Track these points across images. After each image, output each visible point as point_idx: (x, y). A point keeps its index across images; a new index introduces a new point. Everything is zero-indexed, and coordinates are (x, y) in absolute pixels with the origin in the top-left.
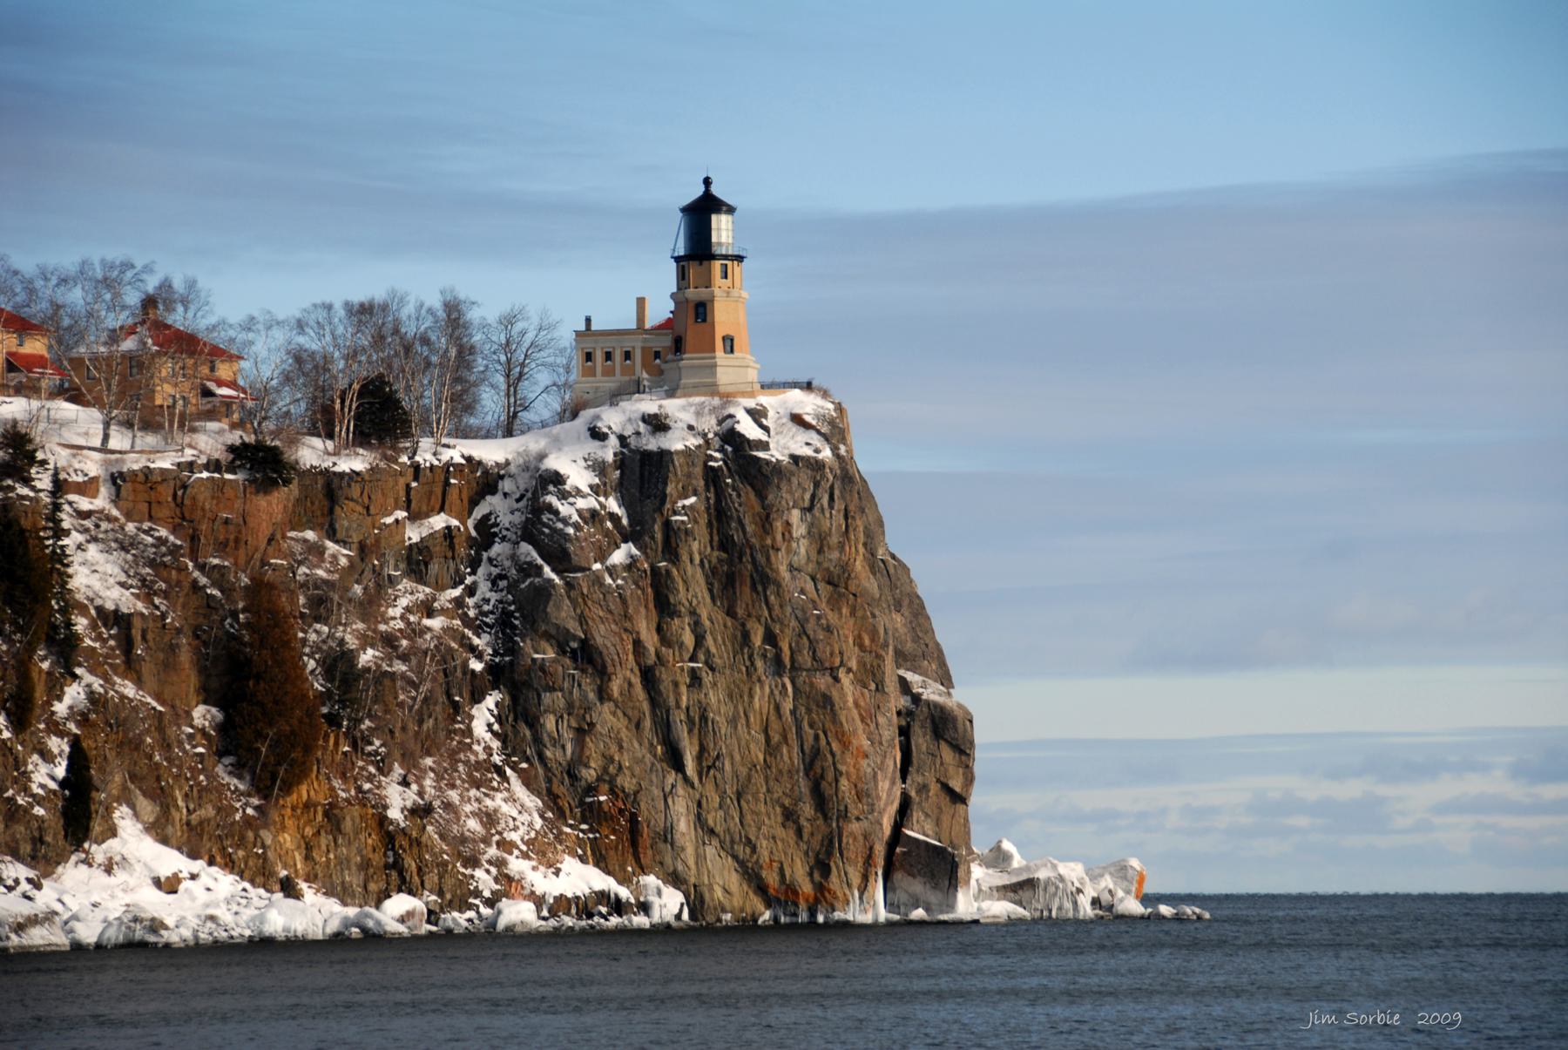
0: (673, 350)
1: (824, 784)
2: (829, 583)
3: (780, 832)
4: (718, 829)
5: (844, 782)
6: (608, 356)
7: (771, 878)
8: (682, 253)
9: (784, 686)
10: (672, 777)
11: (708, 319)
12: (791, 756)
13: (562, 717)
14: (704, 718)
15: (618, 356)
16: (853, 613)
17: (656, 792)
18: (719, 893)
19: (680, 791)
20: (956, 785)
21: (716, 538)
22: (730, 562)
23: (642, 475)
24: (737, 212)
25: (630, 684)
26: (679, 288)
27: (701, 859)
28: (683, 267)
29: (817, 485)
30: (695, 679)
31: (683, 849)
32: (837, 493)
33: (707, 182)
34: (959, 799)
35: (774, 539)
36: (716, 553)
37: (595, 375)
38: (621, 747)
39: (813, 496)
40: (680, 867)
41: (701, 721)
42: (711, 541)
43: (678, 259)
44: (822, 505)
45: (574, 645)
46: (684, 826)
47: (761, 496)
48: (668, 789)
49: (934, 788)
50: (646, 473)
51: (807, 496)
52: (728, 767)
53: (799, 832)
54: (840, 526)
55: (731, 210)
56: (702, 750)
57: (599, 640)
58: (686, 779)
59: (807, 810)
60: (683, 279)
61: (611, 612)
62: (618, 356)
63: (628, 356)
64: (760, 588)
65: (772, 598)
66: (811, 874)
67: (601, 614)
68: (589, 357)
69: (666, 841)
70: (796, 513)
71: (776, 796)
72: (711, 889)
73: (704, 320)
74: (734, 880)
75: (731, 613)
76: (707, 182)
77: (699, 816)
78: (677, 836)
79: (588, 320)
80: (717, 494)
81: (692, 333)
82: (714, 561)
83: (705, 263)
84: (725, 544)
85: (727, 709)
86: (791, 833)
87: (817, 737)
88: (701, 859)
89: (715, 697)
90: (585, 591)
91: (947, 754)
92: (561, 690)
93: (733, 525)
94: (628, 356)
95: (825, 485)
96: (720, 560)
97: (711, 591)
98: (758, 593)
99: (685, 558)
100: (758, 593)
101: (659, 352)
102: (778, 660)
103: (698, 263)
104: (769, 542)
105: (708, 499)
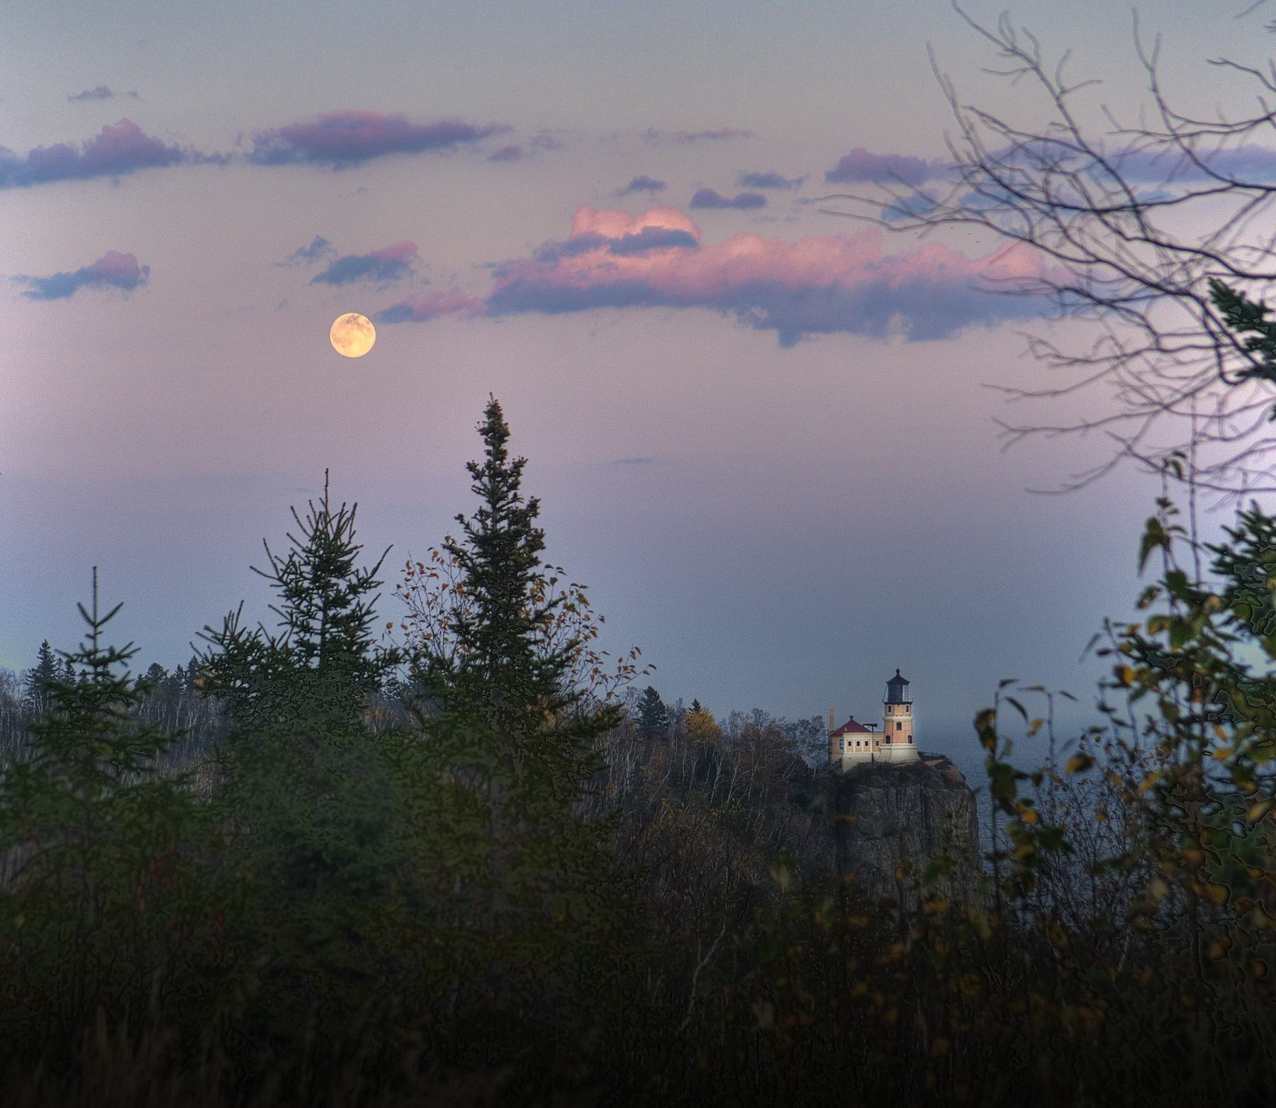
0: (885, 741)
6: (858, 744)
8: (887, 701)
15: (862, 744)
33: (898, 671)
36: (924, 831)
43: (886, 703)
50: (899, 798)
62: (862, 744)
63: (867, 744)
76: (898, 671)
83: (901, 705)
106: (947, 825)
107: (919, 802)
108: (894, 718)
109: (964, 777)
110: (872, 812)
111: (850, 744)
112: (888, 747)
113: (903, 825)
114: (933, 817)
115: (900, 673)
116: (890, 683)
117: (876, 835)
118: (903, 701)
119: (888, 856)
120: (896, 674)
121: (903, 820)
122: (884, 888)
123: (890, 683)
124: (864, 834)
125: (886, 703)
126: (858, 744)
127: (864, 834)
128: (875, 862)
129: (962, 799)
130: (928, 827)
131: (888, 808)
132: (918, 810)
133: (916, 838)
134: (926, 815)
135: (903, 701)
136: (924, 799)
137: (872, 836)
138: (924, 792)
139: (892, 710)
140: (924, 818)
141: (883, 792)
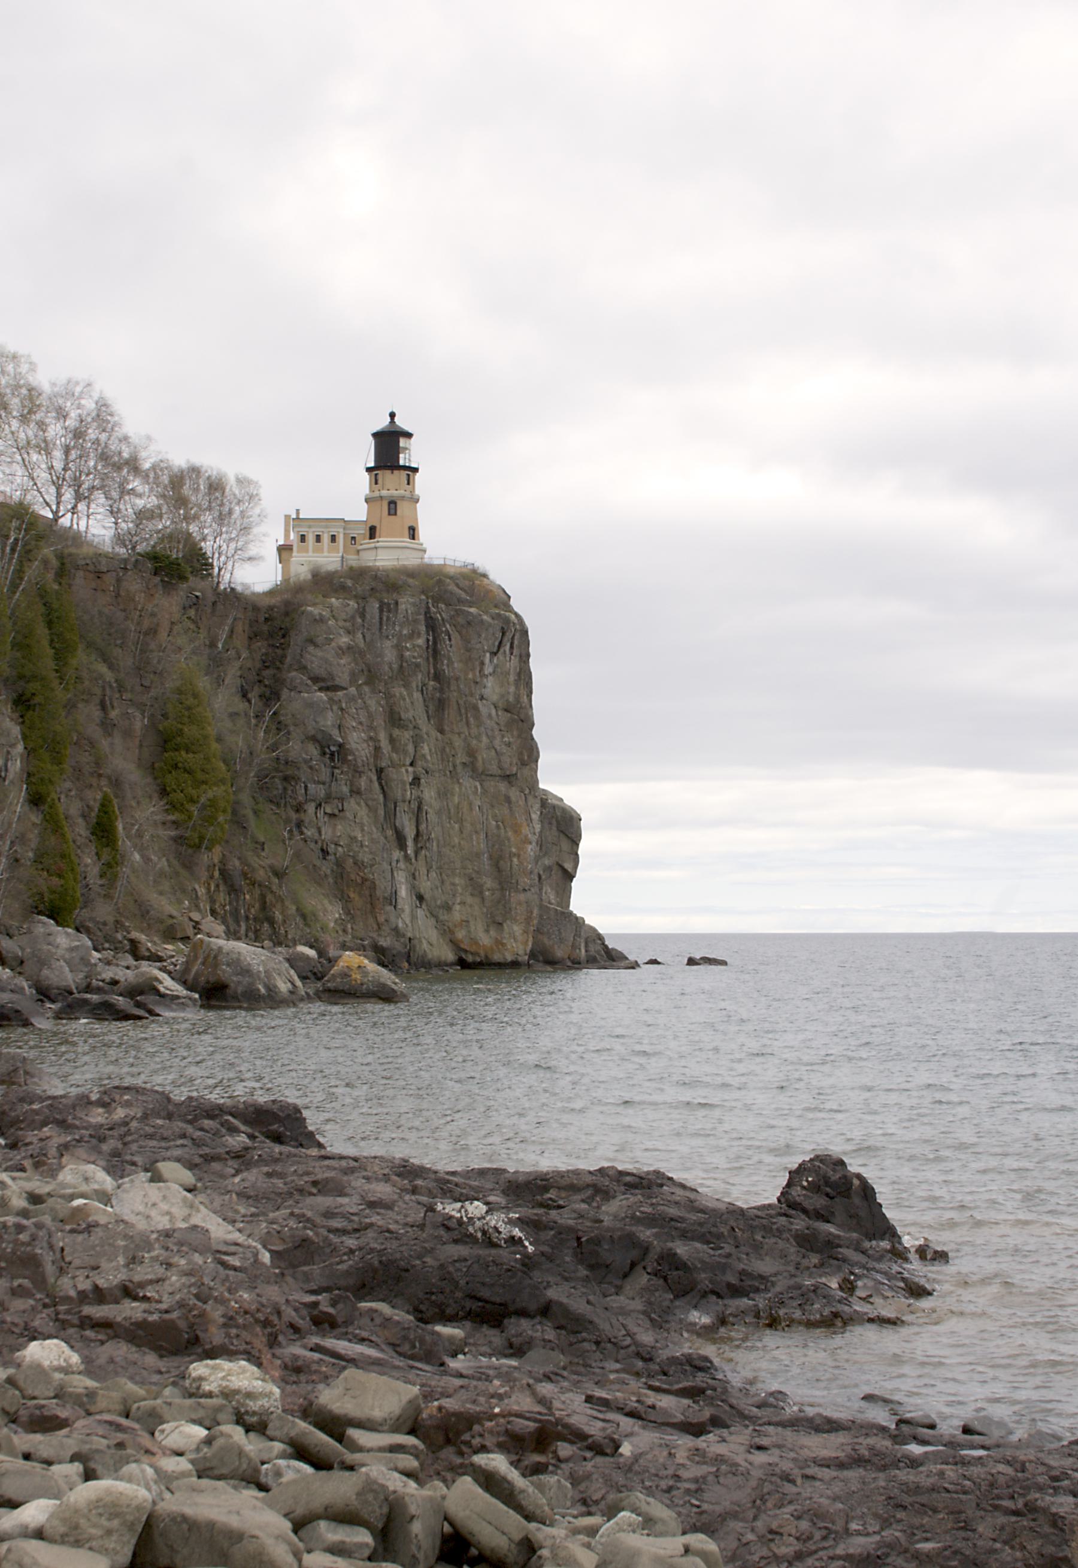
1: (502, 862)
2: (506, 710)
3: (469, 900)
4: (427, 896)
5: (515, 860)
6: (318, 539)
7: (460, 934)
8: (372, 464)
9: (476, 787)
10: (397, 854)
11: (399, 512)
12: (480, 843)
13: (320, 805)
14: (419, 808)
15: (326, 539)
16: (519, 736)
17: (386, 866)
18: (425, 945)
19: (402, 865)
20: (568, 866)
21: (432, 671)
22: (441, 691)
23: (381, 619)
24: (413, 439)
25: (371, 781)
26: (372, 490)
27: (414, 917)
28: (376, 475)
29: (504, 634)
30: (416, 781)
31: (403, 910)
32: (516, 642)
33: (392, 415)
34: (569, 876)
35: (474, 675)
36: (432, 683)
37: (307, 551)
38: (363, 830)
39: (500, 643)
40: (400, 925)
41: (419, 813)
42: (429, 673)
43: (369, 470)
44: (505, 651)
45: (333, 748)
46: (403, 892)
47: (466, 640)
48: (394, 864)
49: (555, 868)
50: (385, 618)
51: (497, 644)
52: (435, 848)
53: (483, 899)
54: (515, 668)
55: (409, 435)
56: (418, 834)
57: (354, 746)
58: (406, 857)
59: (489, 883)
60: (376, 483)
61: (361, 723)
62: (326, 539)
63: (333, 538)
64: (463, 711)
65: (471, 720)
66: (487, 931)
67: (354, 724)
68: (303, 538)
69: (391, 904)
70: (488, 655)
71: (467, 871)
72: (421, 942)
73: (395, 514)
74: (433, 935)
75: (442, 731)
76: (392, 415)
77: (413, 887)
78: (399, 901)
79: (298, 511)
80: (434, 638)
81: (386, 523)
82: (430, 688)
83: (396, 472)
84: (438, 677)
85: (436, 804)
86: (477, 900)
87: (498, 827)
88: (414, 917)
89: (429, 794)
90: (344, 705)
91: (565, 845)
92: (324, 784)
93: (446, 662)
94: (333, 538)
95: (509, 635)
96: (435, 689)
97: (427, 712)
98: (461, 715)
99: (414, 685)
100: (461, 715)
101: (353, 538)
102: (474, 769)
103: (389, 472)
104: (470, 676)
105: (428, 640)
106: (474, 675)
107: (423, 628)
108: (384, 493)
109: (509, 597)
110: (332, 640)
111: (303, 538)
112: (373, 545)
113: (391, 668)
114: (449, 659)
115: (396, 419)
116: (376, 435)
117: (338, 682)
118: (401, 463)
119: (361, 723)
120: (389, 419)
121: (390, 655)
122: (351, 785)
123: (379, 437)
124: (316, 679)
125: (369, 470)
126: (318, 539)
127: (316, 679)
128: (335, 733)
129: (503, 628)
130: (438, 677)
131: (364, 636)
132: (421, 641)
133: (417, 695)
134: (434, 651)
135: (401, 463)
136: (432, 625)
137: (329, 684)
138: (433, 610)
139: (380, 481)
140: (431, 659)
141: (356, 605)
